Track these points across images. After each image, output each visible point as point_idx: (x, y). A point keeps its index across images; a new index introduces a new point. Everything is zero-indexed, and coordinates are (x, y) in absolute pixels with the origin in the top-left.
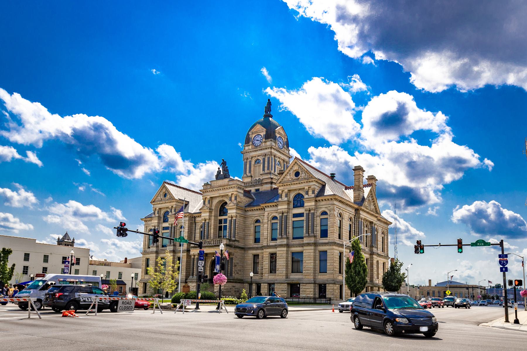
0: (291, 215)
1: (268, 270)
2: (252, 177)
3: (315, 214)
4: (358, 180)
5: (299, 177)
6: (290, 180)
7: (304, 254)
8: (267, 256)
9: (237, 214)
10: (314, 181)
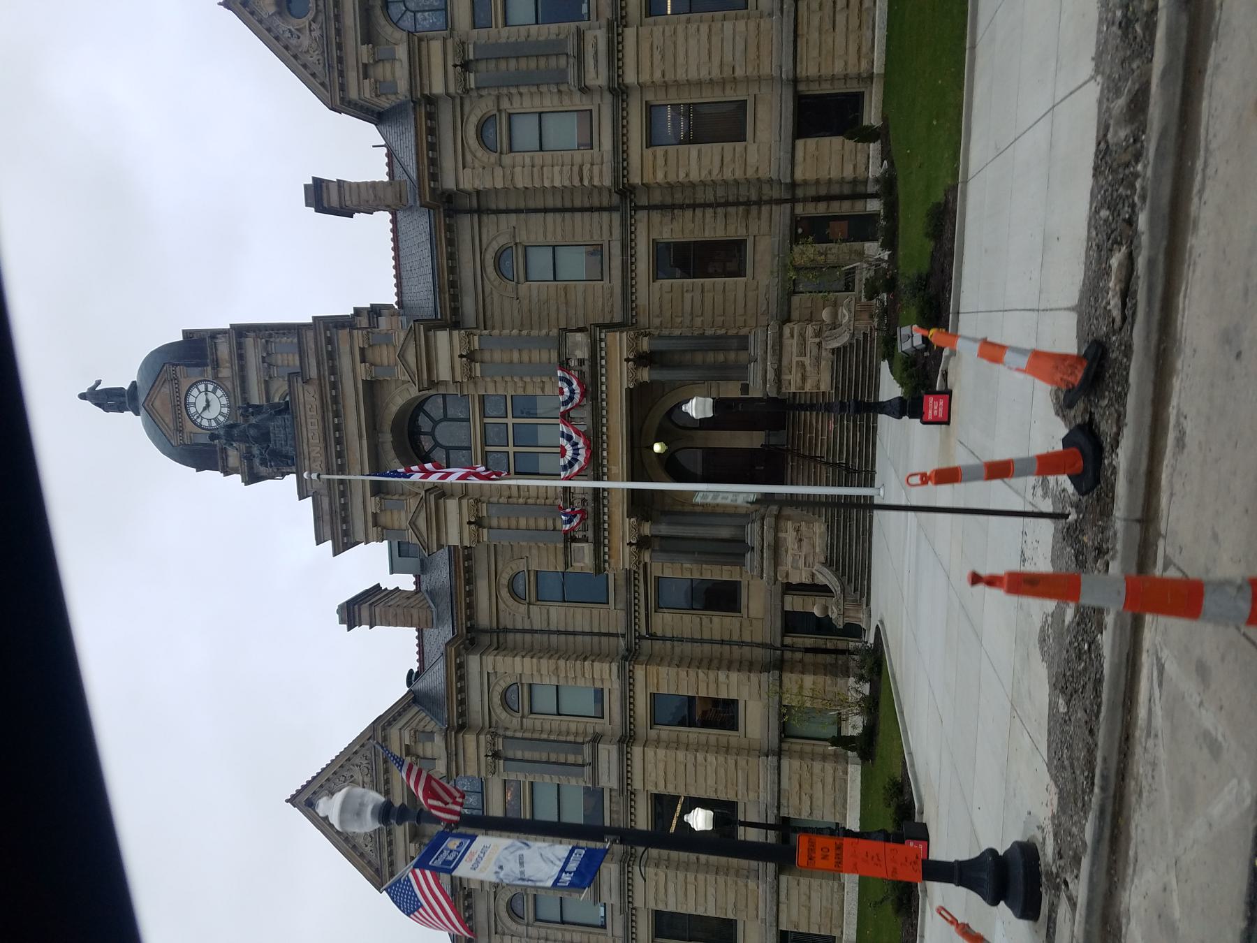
6: (316, 34)
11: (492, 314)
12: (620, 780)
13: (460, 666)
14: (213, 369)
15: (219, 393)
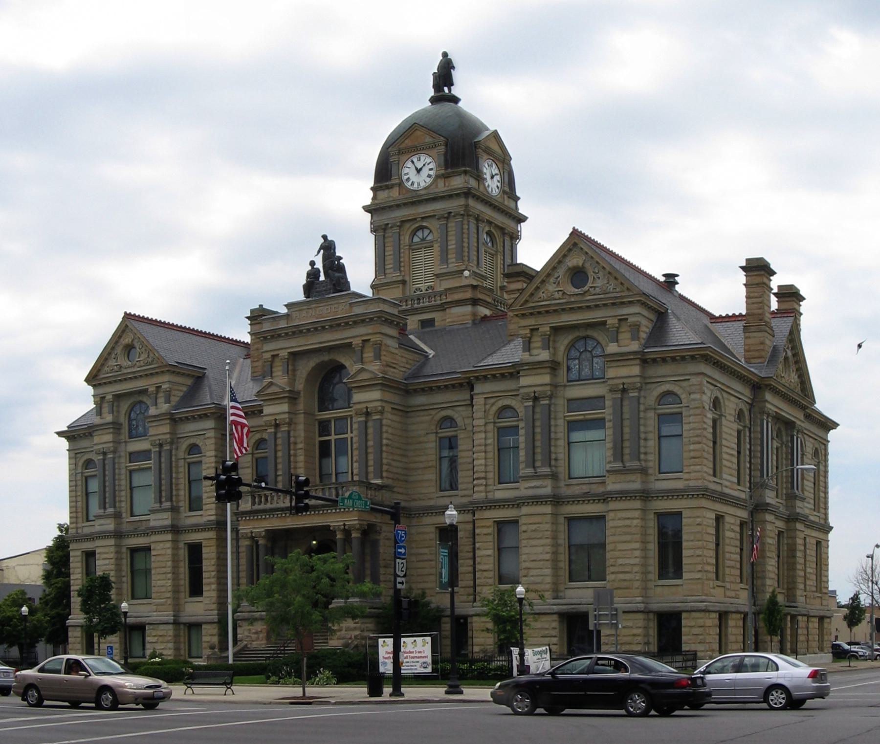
0: (560, 404)
1: (491, 574)
2: (404, 282)
3: (642, 400)
4: (760, 300)
5: (586, 288)
7: (610, 524)
8: (485, 531)
9: (384, 404)
10: (638, 301)
11: (419, 416)
12: (153, 528)
13: (206, 416)
14: (443, 175)
15: (429, 180)
